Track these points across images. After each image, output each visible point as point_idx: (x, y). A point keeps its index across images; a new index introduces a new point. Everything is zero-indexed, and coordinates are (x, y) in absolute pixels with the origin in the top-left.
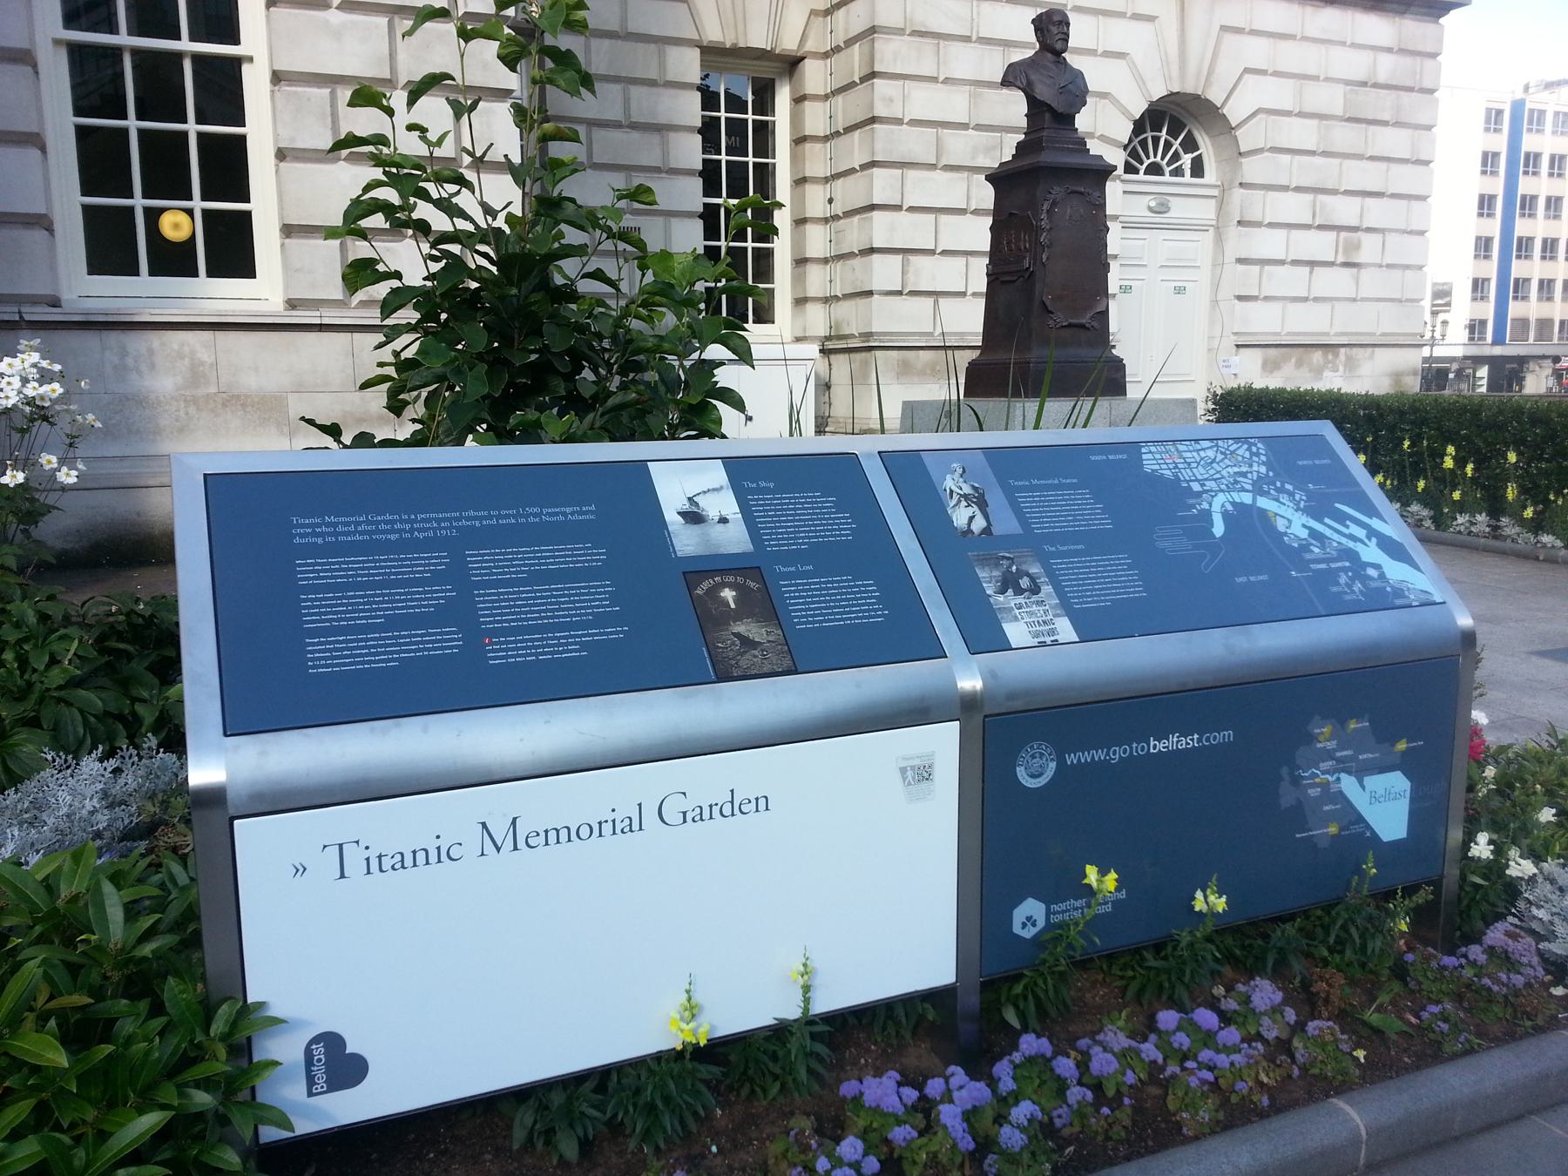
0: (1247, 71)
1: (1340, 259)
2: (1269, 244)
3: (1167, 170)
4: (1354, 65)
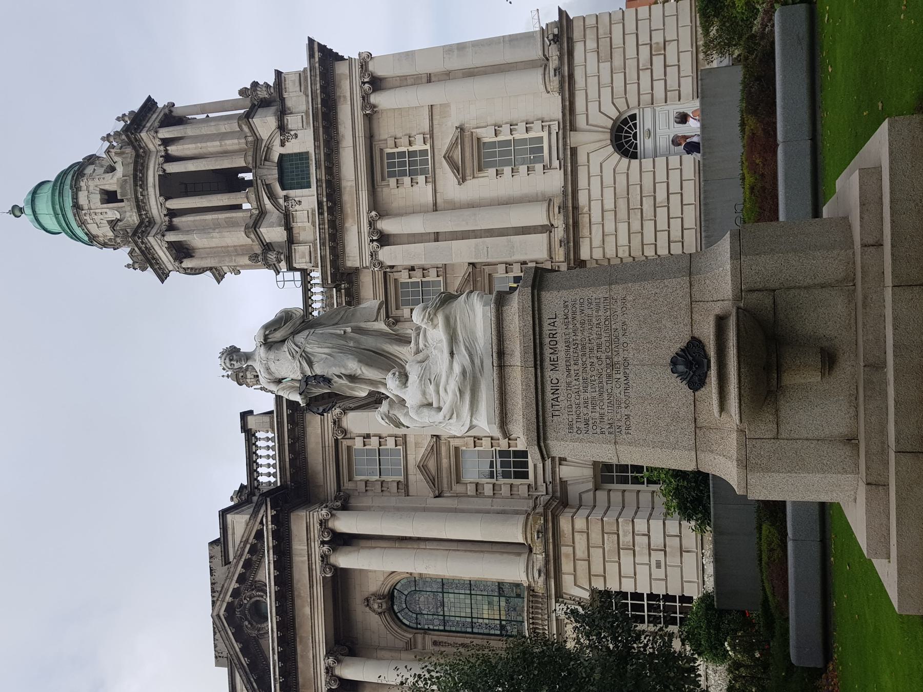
2: (659, 86)
4: (592, 58)
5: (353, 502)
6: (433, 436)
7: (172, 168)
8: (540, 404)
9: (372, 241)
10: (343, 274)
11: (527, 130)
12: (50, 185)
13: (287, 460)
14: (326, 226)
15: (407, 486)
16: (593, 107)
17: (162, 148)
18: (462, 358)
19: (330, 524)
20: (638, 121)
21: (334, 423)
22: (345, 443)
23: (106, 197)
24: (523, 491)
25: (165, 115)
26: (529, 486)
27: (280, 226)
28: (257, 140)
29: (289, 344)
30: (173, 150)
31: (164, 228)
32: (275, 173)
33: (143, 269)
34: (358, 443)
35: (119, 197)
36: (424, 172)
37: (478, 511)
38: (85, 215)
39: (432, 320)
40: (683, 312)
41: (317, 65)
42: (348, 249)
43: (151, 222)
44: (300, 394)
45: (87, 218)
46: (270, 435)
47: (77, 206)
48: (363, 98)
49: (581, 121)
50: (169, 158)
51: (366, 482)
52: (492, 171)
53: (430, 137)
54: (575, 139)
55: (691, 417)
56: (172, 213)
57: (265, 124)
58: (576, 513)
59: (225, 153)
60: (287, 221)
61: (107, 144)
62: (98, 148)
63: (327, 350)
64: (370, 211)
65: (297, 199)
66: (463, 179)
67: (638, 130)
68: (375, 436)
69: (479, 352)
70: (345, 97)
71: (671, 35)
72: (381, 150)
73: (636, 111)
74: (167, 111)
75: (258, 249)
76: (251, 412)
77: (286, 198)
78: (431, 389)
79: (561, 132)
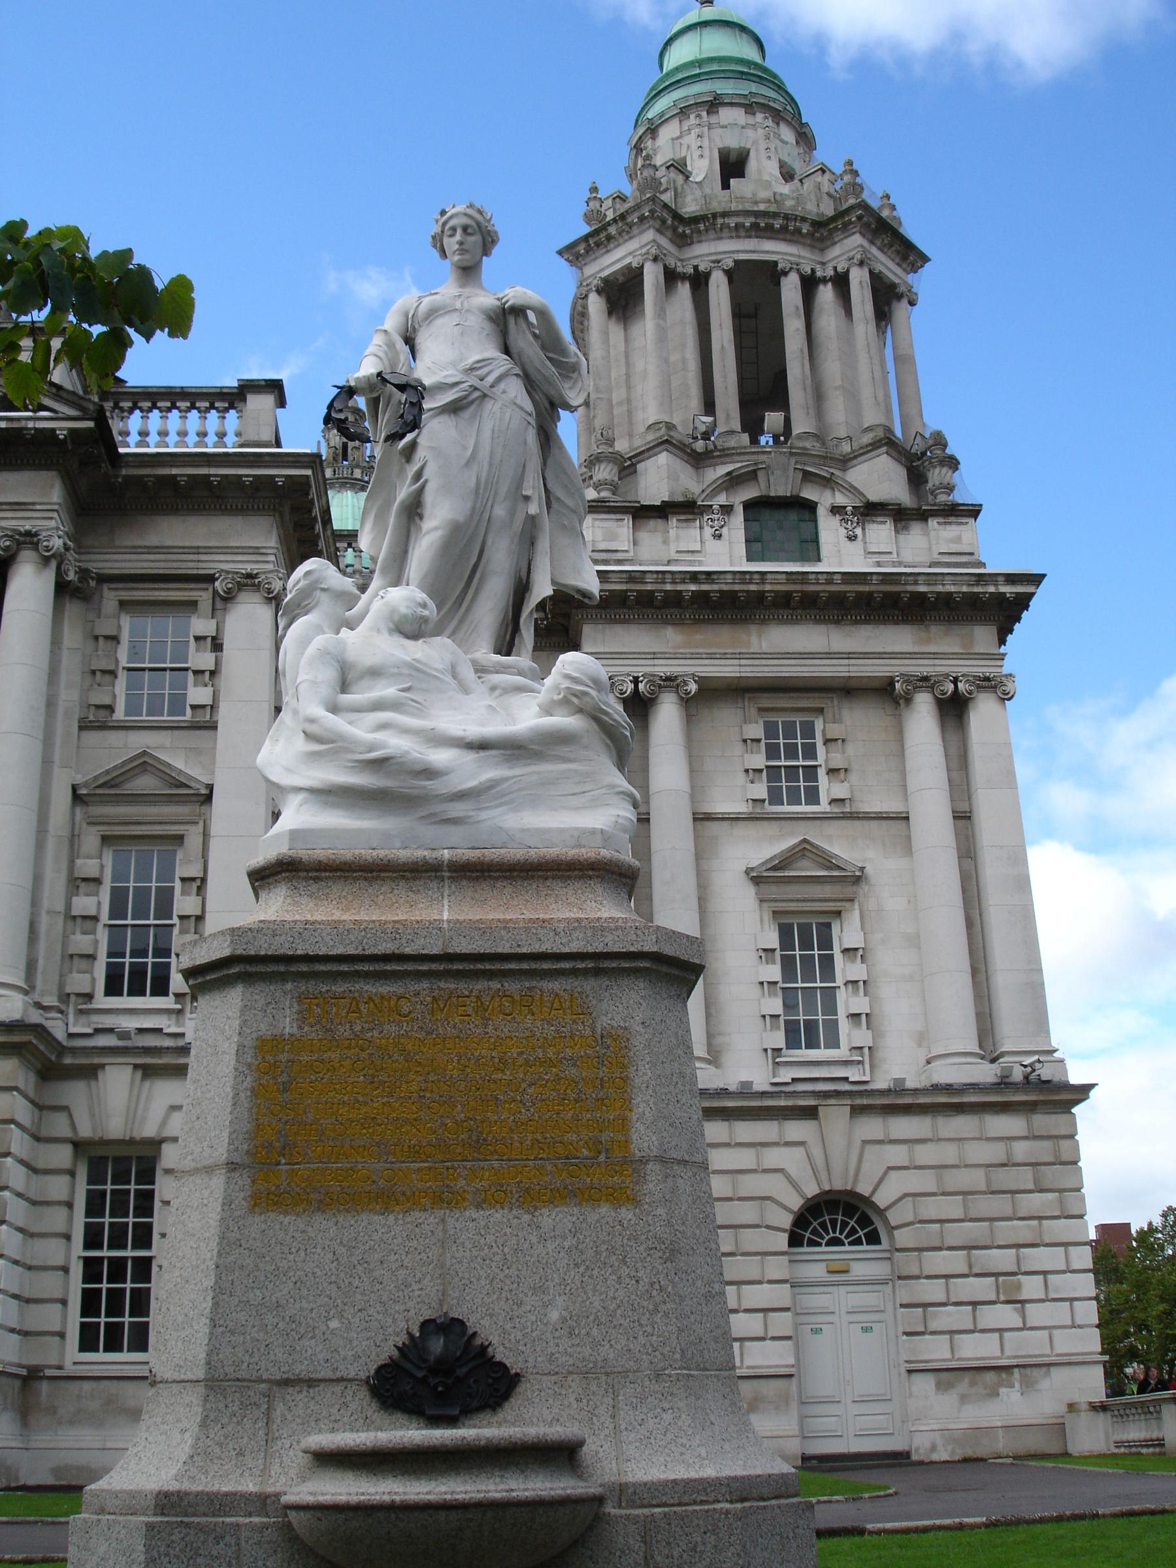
0: (890, 1168)
1: (1002, 1298)
2: (933, 1291)
3: (846, 1242)
5: (73, 609)
6: (210, 787)
7: (790, 291)
8: (344, 968)
9: (636, 681)
10: (567, 616)
11: (855, 1017)
12: (757, 59)
13: (174, 471)
14: (669, 587)
15: (103, 727)
16: (897, 1155)
17: (830, 272)
18: (470, 771)
19: (27, 555)
20: (865, 1247)
21: (250, 576)
22: (204, 597)
23: (733, 157)
24: (78, 982)
25: (893, 286)
26: (89, 997)
27: (671, 494)
28: (845, 462)
29: (503, 363)
30: (826, 294)
31: (671, 262)
32: (781, 488)
33: (588, 218)
34: (202, 625)
35: (733, 182)
36: (775, 797)
37: (38, 879)
38: (699, 116)
39: (565, 702)
40: (587, 1351)
41: (992, 589)
42: (619, 629)
43: (682, 241)
44: (379, 374)
45: (693, 120)
46: (230, 439)
47: (714, 104)
48: (925, 679)
49: (872, 1127)
50: (809, 284)
51: (115, 639)
52: (772, 939)
53: (847, 813)
54: (836, 1117)
55: (301, 1369)
56: (699, 281)
57: (880, 478)
58: (26, 1097)
59: (818, 396)
60: (684, 509)
61: (838, 168)
62: (829, 153)
63: (484, 454)
64: (701, 681)
65: (725, 531)
66: (757, 879)
67: (847, 1248)
68: (218, 662)
69: (484, 815)
70: (928, 641)
71: (1037, 1314)
72: (820, 711)
73: (885, 1243)
74: (902, 289)
75: (622, 446)
76: (282, 403)
77: (727, 510)
78: (387, 690)
79: (847, 1087)
